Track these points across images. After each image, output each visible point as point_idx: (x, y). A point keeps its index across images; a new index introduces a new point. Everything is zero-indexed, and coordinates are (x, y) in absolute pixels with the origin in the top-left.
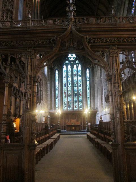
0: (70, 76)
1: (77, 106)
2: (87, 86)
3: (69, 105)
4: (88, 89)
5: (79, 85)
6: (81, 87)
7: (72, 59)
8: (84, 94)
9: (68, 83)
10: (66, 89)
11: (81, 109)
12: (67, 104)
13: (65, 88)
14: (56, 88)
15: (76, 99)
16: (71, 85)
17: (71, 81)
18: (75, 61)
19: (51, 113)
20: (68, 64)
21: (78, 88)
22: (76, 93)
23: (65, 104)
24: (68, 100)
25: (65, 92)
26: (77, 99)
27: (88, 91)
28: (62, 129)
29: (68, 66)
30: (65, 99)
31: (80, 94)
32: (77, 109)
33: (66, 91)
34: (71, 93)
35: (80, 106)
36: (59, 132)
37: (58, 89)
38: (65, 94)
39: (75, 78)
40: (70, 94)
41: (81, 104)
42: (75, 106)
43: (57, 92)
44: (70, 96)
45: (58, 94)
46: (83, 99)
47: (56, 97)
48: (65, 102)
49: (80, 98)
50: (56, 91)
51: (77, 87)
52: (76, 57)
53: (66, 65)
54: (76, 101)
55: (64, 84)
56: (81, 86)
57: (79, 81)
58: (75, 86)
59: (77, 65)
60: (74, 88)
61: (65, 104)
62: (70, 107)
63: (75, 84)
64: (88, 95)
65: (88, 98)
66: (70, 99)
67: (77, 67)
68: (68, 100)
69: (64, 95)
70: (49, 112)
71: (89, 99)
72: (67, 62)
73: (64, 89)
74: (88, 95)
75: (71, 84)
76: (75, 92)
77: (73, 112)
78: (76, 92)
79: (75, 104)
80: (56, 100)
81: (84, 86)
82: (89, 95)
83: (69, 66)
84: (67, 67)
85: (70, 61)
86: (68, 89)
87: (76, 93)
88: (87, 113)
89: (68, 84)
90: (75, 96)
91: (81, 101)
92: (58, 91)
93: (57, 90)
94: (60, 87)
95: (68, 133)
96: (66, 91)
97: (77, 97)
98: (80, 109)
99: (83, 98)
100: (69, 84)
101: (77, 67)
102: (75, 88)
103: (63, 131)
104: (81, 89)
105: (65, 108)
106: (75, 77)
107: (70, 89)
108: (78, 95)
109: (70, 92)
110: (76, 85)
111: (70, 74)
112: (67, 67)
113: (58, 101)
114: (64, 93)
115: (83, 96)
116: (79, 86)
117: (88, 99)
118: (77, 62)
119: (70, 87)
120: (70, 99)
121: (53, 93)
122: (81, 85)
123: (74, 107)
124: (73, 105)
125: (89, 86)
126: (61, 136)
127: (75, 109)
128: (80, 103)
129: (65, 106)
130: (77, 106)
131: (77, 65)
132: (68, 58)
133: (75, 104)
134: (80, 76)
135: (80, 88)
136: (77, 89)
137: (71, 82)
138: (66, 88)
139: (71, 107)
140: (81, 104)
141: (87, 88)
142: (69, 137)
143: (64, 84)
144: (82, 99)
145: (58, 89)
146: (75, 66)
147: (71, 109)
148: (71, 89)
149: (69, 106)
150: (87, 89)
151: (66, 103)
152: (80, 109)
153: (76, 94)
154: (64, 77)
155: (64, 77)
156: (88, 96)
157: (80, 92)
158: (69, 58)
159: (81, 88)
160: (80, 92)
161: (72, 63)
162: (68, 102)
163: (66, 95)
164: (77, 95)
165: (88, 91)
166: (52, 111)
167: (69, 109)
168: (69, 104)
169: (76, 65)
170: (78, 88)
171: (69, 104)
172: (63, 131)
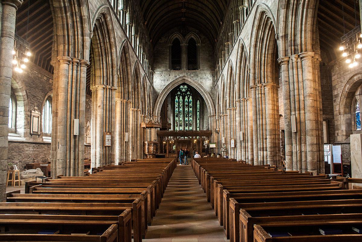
7: (184, 90)
18: (186, 92)
20: (180, 95)
26: (188, 129)
29: (180, 97)
52: (188, 89)
53: (178, 96)
59: (189, 96)
60: (185, 118)
67: (189, 98)
72: (179, 93)
75: (182, 115)
76: (186, 122)
78: (187, 122)
83: (181, 97)
84: (179, 98)
85: (181, 92)
86: (180, 119)
90: (186, 126)
100: (181, 115)
101: (189, 98)
102: (186, 119)
106: (186, 108)
111: (181, 105)
112: (179, 98)
118: (188, 93)
131: (189, 96)
132: (180, 89)
136: (187, 119)
146: (186, 97)
148: (182, 119)
153: (187, 124)
154: (176, 108)
158: (181, 89)
161: (184, 94)
169: (188, 96)
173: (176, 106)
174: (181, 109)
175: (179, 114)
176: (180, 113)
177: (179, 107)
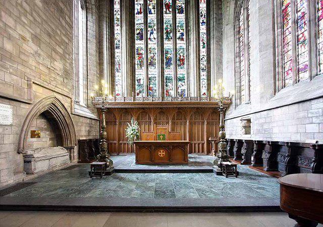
0: (153, 11)
2: (201, 39)
5: (178, 35)
6: (182, 39)
9: (149, 29)
10: (143, 46)
12: (145, 84)
13: (139, 44)
15: (169, 72)
16: (155, 35)
17: (155, 22)
24: (149, 76)
25: (141, 54)
26: (173, 73)
30: (140, 73)
31: (180, 60)
33: (143, 52)
35: (180, 91)
39: (168, 17)
40: (152, 58)
41: (183, 87)
44: (152, 64)
46: (188, 74)
47: (117, 66)
49: (182, 72)
51: (171, 42)
54: (168, 79)
56: (184, 37)
57: (177, 25)
58: (168, 38)
60: (165, 42)
63: (167, 32)
66: (154, 71)
68: (149, 76)
69: (137, 61)
71: (205, 73)
73: (136, 46)
75: (155, 32)
79: (166, 86)
80: (117, 74)
82: (205, 63)
87: (169, 55)
89: (149, 33)
90: (168, 64)
96: (143, 52)
97: (172, 67)
100: (152, 33)
102: (168, 45)
104: (184, 46)
107: (153, 45)
116: (179, 38)
117: (202, 73)
122: (182, 34)
128: (180, 83)
129: (140, 92)
133: (166, 86)
134: (181, 12)
137: (155, 27)
138: (143, 42)
140: (185, 87)
141: (201, 44)
143: (138, 31)
144: (185, 73)
148: (156, 46)
150: (201, 47)
151: (142, 82)
153: (169, 60)
155: (136, 11)
156: (201, 65)
157: (182, 54)
159: (185, 42)
164: (172, 62)
165: (203, 51)
168: (151, 86)
171: (151, 86)
173: (137, 7)
174: (152, 17)
176: (150, 27)
177: (146, 11)
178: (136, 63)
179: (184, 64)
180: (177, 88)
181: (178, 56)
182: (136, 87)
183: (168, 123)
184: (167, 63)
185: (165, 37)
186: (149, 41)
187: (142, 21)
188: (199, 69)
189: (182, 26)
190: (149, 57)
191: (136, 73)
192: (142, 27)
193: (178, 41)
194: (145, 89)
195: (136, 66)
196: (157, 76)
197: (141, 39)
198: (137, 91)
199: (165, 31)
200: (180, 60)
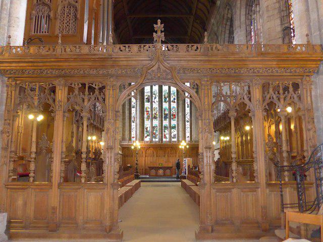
1: (168, 136)
2: (186, 102)
3: (155, 134)
4: (188, 107)
5: (172, 99)
6: (175, 102)
8: (180, 114)
9: (154, 96)
10: (150, 107)
11: (175, 140)
13: (147, 105)
14: (132, 103)
15: (166, 123)
16: (157, 99)
17: (158, 91)
19: (124, 146)
21: (170, 105)
22: (166, 112)
23: (147, 131)
24: (153, 125)
25: (148, 111)
26: (168, 124)
27: (188, 110)
28: (142, 174)
30: (147, 124)
31: (173, 115)
32: (168, 140)
34: (158, 113)
35: (172, 135)
36: (137, 177)
37: (136, 105)
38: (147, 114)
40: (155, 114)
41: (174, 132)
42: (165, 135)
43: (133, 110)
44: (155, 118)
45: (136, 114)
46: (178, 124)
47: (133, 119)
48: (147, 128)
49: (174, 123)
50: (133, 109)
51: (168, 104)
54: (165, 127)
55: (146, 97)
56: (176, 101)
57: (171, 93)
58: (165, 101)
60: (164, 103)
61: (147, 131)
62: (155, 137)
64: (188, 117)
65: (188, 121)
66: (156, 122)
68: (153, 125)
69: (146, 116)
70: (121, 145)
71: (189, 123)
73: (145, 106)
74: (188, 117)
75: (157, 98)
77: (161, 145)
78: (167, 112)
80: (133, 124)
81: (181, 102)
82: (189, 117)
87: (166, 112)
88: (183, 147)
89: (153, 98)
90: (165, 118)
91: (174, 127)
92: (136, 109)
93: (134, 107)
94: (138, 103)
95: (152, 180)
96: (149, 110)
97: (168, 119)
98: (173, 140)
99: (178, 121)
100: (155, 98)
102: (165, 105)
103: (144, 176)
104: (176, 107)
105: (147, 139)
107: (156, 105)
108: (170, 116)
109: (156, 111)
110: (168, 99)
113: (136, 126)
114: (145, 112)
115: (178, 119)
117: (187, 123)
119: (156, 102)
120: (156, 122)
121: (127, 112)
122: (174, 99)
123: (162, 136)
124: (162, 134)
125: (189, 104)
126: (142, 184)
127: (164, 140)
128: (172, 130)
129: (148, 136)
130: (168, 136)
135: (174, 105)
137: (158, 94)
139: (157, 137)
140: (176, 133)
142: (152, 186)
143: (147, 97)
144: (176, 124)
145: (136, 105)
147: (157, 140)
148: (157, 106)
149: (153, 135)
150: (186, 107)
151: (148, 129)
152: (173, 140)
153: (166, 115)
156: (186, 118)
159: (176, 104)
160: (174, 111)
162: (153, 128)
163: (148, 117)
165: (188, 110)
166: (125, 143)
167: (154, 140)
168: (155, 132)
170: (170, 105)
171: (155, 132)
172: (144, 176)
175: (152, 96)
178: (145, 117)
179: (175, 117)
180: (170, 133)
181: (172, 113)
182: (145, 132)
183: (165, 156)
184: (165, 117)
185: (163, 100)
186: (153, 103)
187: (149, 90)
188: (185, 121)
189: (174, 94)
190: (153, 113)
191: (145, 124)
192: (149, 94)
193: (172, 103)
194: (151, 134)
195: (145, 119)
196: (158, 125)
197: (149, 102)
198: (146, 135)
199: (163, 97)
200: (173, 115)
